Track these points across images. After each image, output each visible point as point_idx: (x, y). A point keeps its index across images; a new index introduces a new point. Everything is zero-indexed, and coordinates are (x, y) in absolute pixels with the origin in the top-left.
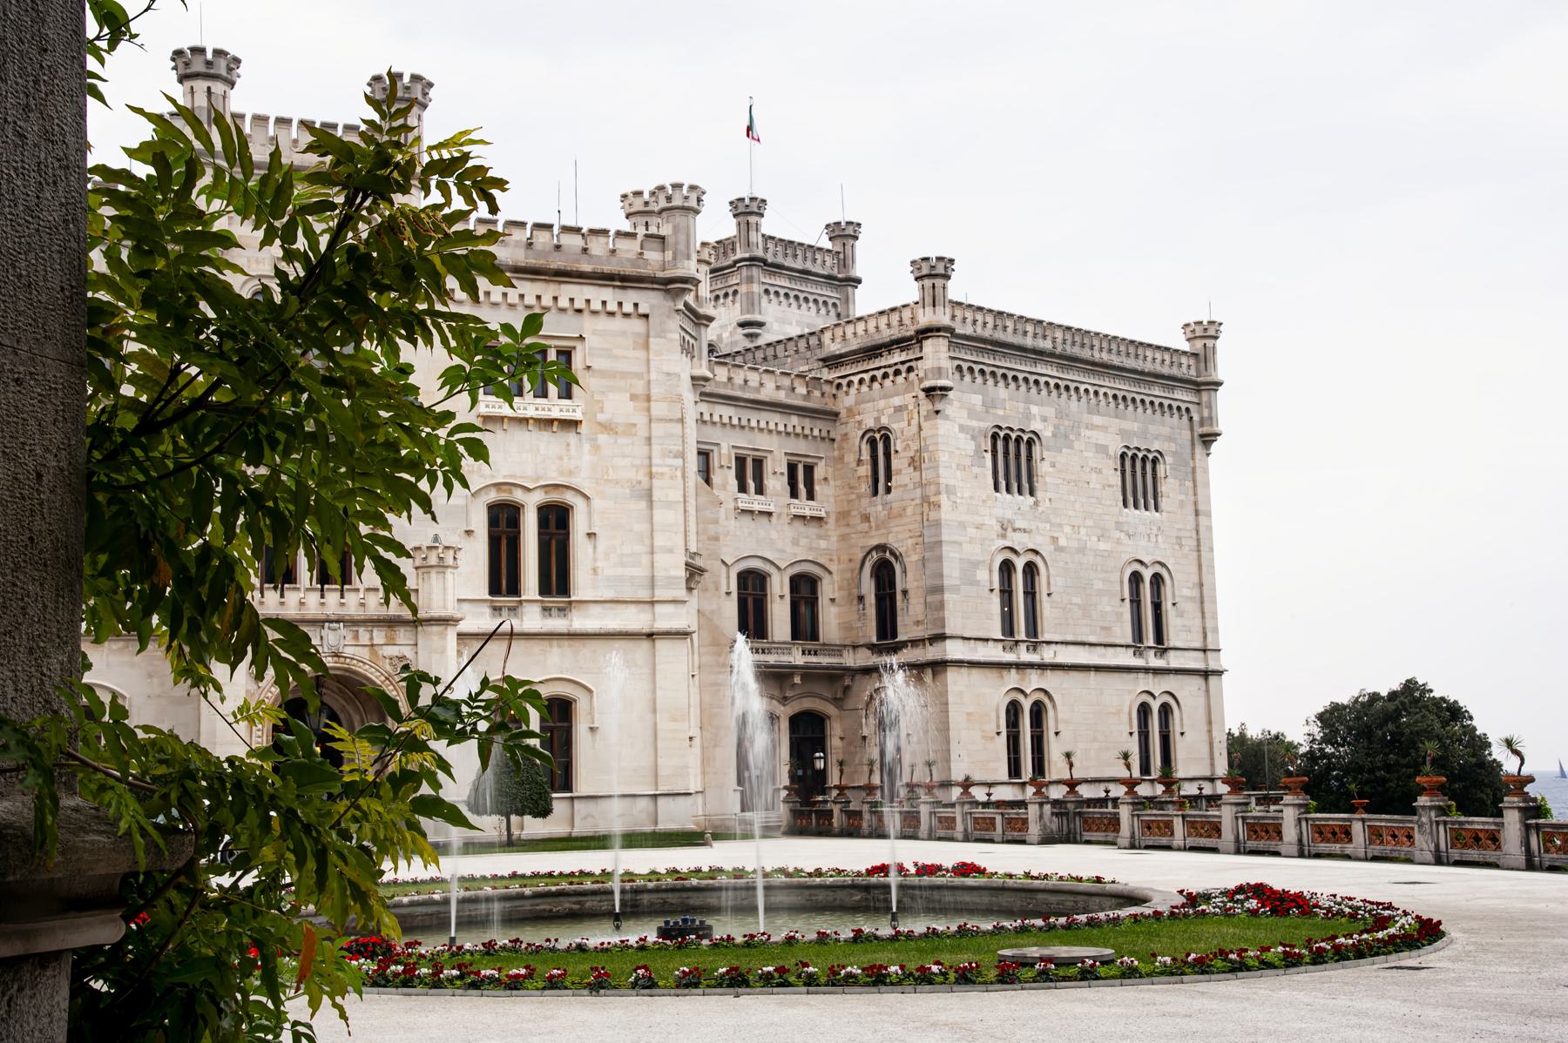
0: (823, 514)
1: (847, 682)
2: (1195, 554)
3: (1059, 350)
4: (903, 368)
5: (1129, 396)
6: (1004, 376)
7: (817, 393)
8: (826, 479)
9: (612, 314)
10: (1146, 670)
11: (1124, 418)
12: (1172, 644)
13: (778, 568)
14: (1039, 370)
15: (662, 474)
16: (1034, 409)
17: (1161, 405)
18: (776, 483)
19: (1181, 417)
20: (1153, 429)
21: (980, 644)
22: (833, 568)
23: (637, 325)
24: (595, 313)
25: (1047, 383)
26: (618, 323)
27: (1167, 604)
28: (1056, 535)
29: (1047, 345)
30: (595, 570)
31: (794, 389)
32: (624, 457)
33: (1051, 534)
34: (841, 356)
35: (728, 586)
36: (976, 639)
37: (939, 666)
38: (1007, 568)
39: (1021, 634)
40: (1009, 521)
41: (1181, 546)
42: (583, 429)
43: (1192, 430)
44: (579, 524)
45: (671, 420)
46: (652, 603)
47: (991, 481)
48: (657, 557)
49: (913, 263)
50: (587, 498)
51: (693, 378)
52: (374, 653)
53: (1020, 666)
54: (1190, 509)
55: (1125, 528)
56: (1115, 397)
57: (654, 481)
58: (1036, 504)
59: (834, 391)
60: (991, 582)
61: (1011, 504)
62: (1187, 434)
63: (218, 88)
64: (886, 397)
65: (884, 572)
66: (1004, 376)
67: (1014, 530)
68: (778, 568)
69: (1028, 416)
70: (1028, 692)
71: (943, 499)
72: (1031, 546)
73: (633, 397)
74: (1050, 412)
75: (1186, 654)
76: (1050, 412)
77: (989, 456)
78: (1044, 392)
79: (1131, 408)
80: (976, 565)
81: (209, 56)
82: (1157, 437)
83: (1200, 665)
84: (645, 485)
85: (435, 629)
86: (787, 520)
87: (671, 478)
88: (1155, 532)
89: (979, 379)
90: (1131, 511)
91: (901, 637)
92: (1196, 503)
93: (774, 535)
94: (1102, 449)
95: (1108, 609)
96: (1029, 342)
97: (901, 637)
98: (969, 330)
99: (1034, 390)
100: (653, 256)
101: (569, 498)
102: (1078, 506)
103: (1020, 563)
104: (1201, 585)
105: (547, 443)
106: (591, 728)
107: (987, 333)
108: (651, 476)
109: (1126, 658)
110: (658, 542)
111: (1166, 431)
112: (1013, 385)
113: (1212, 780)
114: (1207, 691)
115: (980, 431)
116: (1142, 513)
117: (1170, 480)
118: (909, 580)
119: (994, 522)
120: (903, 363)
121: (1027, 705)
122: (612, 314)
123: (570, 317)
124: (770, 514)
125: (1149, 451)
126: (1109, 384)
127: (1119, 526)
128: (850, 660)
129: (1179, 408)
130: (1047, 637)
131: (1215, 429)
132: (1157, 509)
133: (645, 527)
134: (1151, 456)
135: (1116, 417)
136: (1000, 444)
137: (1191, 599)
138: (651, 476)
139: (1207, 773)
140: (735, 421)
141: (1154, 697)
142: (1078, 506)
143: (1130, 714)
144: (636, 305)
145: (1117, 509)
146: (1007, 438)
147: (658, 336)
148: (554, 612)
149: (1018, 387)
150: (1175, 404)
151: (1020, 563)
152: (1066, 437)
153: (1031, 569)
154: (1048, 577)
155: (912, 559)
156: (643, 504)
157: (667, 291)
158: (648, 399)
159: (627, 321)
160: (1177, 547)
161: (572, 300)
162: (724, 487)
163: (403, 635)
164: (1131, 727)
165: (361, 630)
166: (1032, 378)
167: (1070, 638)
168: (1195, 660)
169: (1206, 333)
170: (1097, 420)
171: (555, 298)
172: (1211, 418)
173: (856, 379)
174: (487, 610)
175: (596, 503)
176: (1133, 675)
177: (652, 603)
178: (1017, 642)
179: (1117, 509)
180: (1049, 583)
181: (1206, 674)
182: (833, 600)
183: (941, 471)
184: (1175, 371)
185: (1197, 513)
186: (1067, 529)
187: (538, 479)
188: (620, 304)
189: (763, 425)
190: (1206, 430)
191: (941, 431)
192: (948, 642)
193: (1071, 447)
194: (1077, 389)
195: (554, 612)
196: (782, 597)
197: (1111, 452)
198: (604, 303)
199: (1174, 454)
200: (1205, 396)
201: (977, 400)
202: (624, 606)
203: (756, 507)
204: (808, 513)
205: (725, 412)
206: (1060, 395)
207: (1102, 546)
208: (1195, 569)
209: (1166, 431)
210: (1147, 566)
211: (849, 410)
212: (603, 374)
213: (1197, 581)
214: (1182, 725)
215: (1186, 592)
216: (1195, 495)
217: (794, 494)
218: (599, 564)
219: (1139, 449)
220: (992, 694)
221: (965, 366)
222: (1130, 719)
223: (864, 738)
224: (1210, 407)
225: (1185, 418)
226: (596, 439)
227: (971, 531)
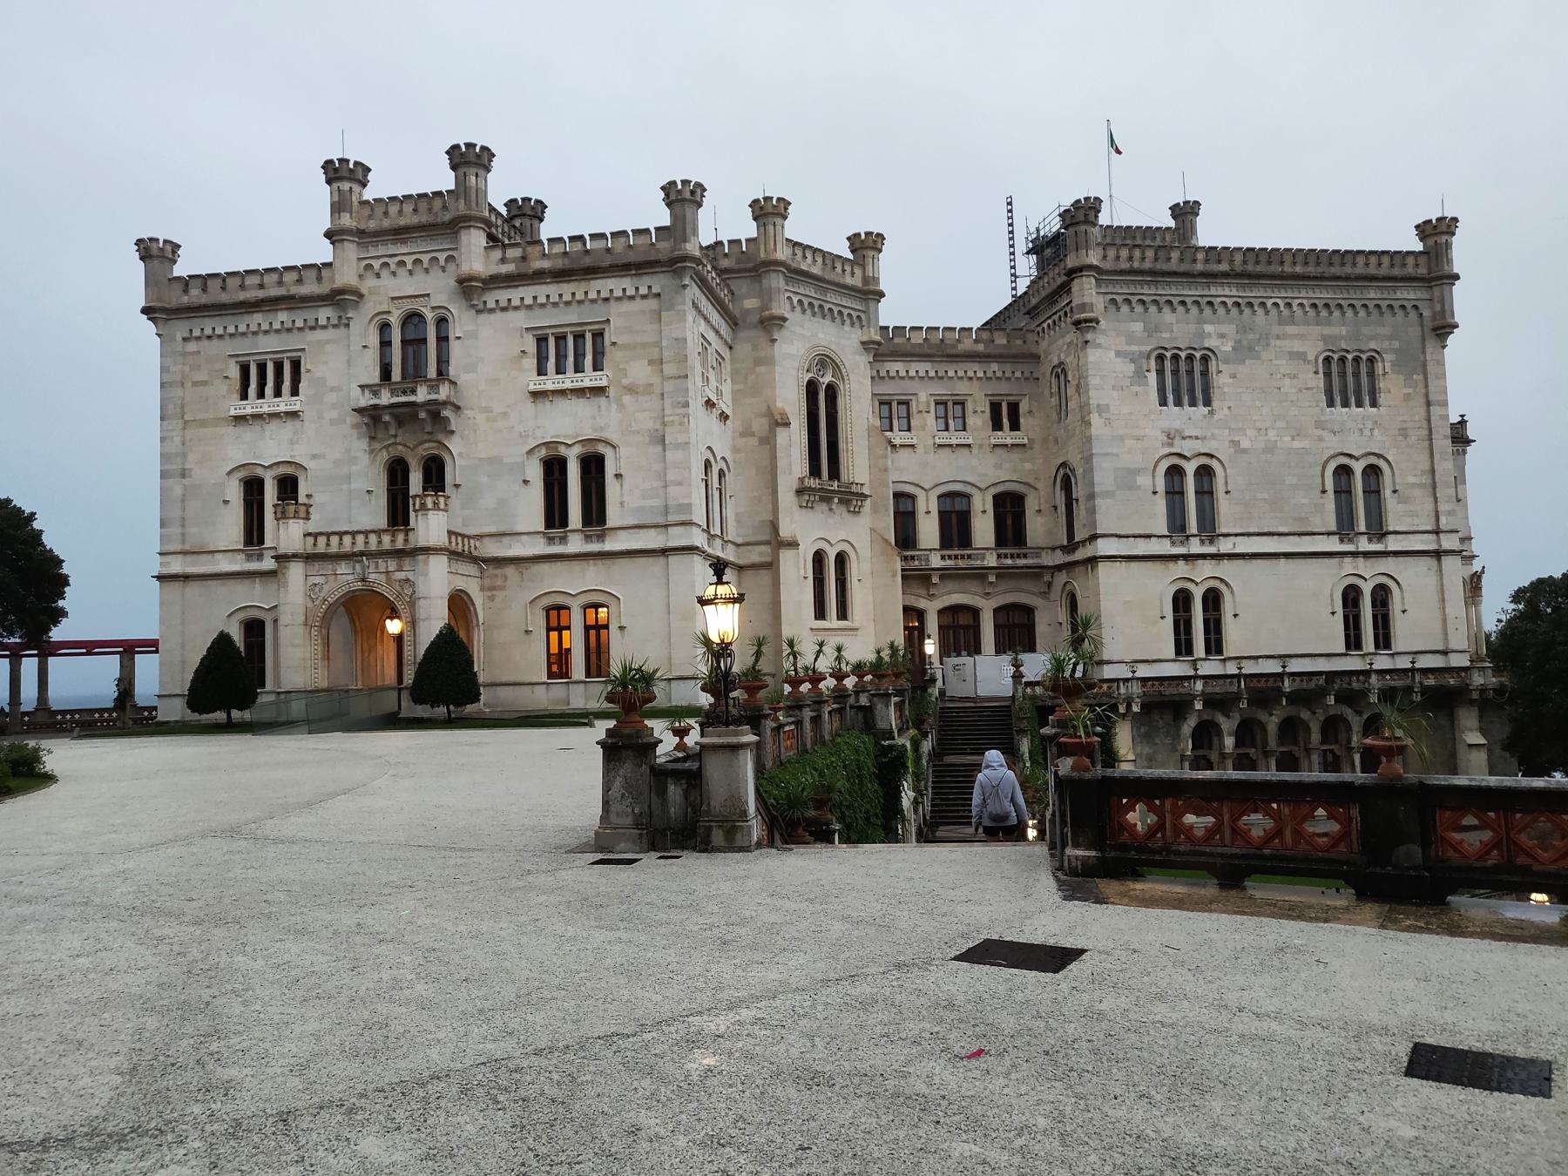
0: (1026, 441)
1: (1047, 578)
2: (1426, 443)
3: (1238, 268)
4: (1068, 309)
5: (1332, 304)
6: (1169, 302)
7: (1019, 342)
8: (1030, 412)
9: (632, 298)
10: (1354, 554)
11: (1329, 324)
12: (1391, 529)
13: (980, 489)
14: (1213, 291)
15: (672, 421)
16: (1208, 328)
17: (1378, 306)
18: (978, 420)
19: (1407, 314)
20: (1366, 330)
21: (1142, 539)
22: (1039, 485)
23: (652, 304)
24: (618, 299)
25: (1224, 303)
26: (638, 305)
27: (1387, 492)
28: (1237, 439)
29: (1224, 267)
30: (622, 504)
31: (993, 341)
32: (642, 414)
33: (1231, 438)
34: (1036, 307)
35: (927, 507)
36: (1134, 537)
37: (1093, 561)
38: (1175, 472)
39: (1193, 526)
40: (1177, 431)
41: (1406, 436)
42: (612, 392)
43: (1422, 326)
44: (610, 469)
45: (679, 377)
46: (666, 526)
47: (1154, 395)
48: (670, 489)
49: (1417, 227)
50: (615, 447)
51: (863, 343)
52: (389, 581)
53: (1188, 558)
54: (1422, 400)
55: (1329, 426)
56: (1314, 306)
57: (666, 428)
58: (1211, 413)
59: (1036, 338)
60: (1154, 486)
61: (1175, 417)
62: (1414, 331)
63: (346, 186)
64: (1063, 336)
65: (1067, 485)
66: (1169, 302)
67: (1184, 438)
68: (980, 489)
69: (1202, 335)
70: (1198, 581)
71: (1095, 419)
72: (1203, 451)
73: (651, 362)
74: (1230, 329)
75: (1411, 536)
76: (1230, 329)
77: (1152, 377)
78: (1221, 311)
79: (1337, 313)
80: (1138, 471)
81: (351, 166)
82: (1373, 338)
83: (1432, 547)
84: (661, 433)
85: (420, 557)
86: (989, 450)
87: (680, 424)
88: (1369, 425)
89: (1139, 309)
90: (1339, 410)
91: (1077, 540)
92: (1427, 395)
93: (975, 462)
94: (1301, 356)
95: (1304, 501)
96: (1199, 267)
97: (1077, 540)
98: (1125, 266)
99: (1207, 311)
100: (664, 245)
101: (602, 449)
102: (1265, 411)
103: (1190, 468)
104: (1433, 471)
105: (582, 407)
106: (622, 628)
107: (1147, 265)
108: (664, 424)
109: (1333, 545)
110: (671, 476)
111: (1386, 330)
112: (1180, 309)
113: (1445, 653)
114: (1441, 571)
115: (1141, 352)
117: (1391, 376)
118: (1079, 492)
119: (1158, 433)
120: (1067, 304)
121: (1198, 593)
122: (632, 298)
123: (600, 306)
124: (969, 446)
125: (1361, 351)
126: (1303, 295)
127: (1320, 425)
128: (1048, 559)
129: (1403, 307)
130: (1224, 530)
131: (1449, 320)
132: (1374, 404)
133: (657, 466)
134: (1364, 357)
135: (1317, 324)
136: (1168, 364)
137: (1420, 486)
138: (664, 424)
139: (1440, 648)
140: (932, 374)
141: (1366, 580)
142: (1265, 411)
143: (1332, 596)
144: (650, 287)
145: (1317, 410)
146: (1176, 357)
147: (668, 309)
148: (594, 539)
149: (1188, 311)
150: (1396, 304)
151: (1190, 468)
152: (1251, 349)
153: (1205, 473)
154: (1226, 477)
155: (1079, 472)
156: (660, 448)
157: (674, 271)
158: (662, 363)
159: (645, 302)
160: (1401, 438)
161: (599, 292)
162: (923, 428)
163: (407, 562)
164: (1333, 606)
165: (380, 561)
166: (1203, 301)
167: (1252, 530)
168: (1422, 542)
169: (1437, 232)
170: (1291, 329)
171: (586, 293)
172: (1443, 311)
173: (1045, 325)
174: (541, 540)
175: (623, 451)
176: (1335, 561)
177: (666, 526)
178: (1188, 537)
179: (1317, 410)
180: (1226, 483)
181: (1438, 554)
182: (1039, 511)
183: (1091, 393)
184: (1397, 271)
185: (1428, 404)
186: (1251, 433)
187: (577, 436)
188: (637, 289)
189: (961, 373)
190: (1439, 323)
191: (1091, 359)
192: (1099, 540)
193: (1259, 358)
194: (1263, 304)
195: (557, 540)
196: (984, 512)
197: (1311, 357)
198: (624, 290)
199: (1396, 351)
200: (1436, 291)
201: (1137, 327)
202: (645, 530)
203: (954, 441)
204: (1009, 441)
205: (922, 367)
206: (1241, 312)
207: (1297, 444)
208: (1425, 457)
209: (1386, 330)
210: (1357, 459)
211: (1045, 351)
212: (626, 347)
213: (1427, 466)
214: (1403, 604)
215: (1412, 479)
216: (1426, 386)
217: (997, 425)
218: (625, 499)
219: (1348, 351)
220: (1160, 585)
221: (1119, 299)
222: (1332, 600)
223: (1061, 624)
224: (1442, 301)
225: (1413, 315)
226: (621, 400)
227: (1129, 443)
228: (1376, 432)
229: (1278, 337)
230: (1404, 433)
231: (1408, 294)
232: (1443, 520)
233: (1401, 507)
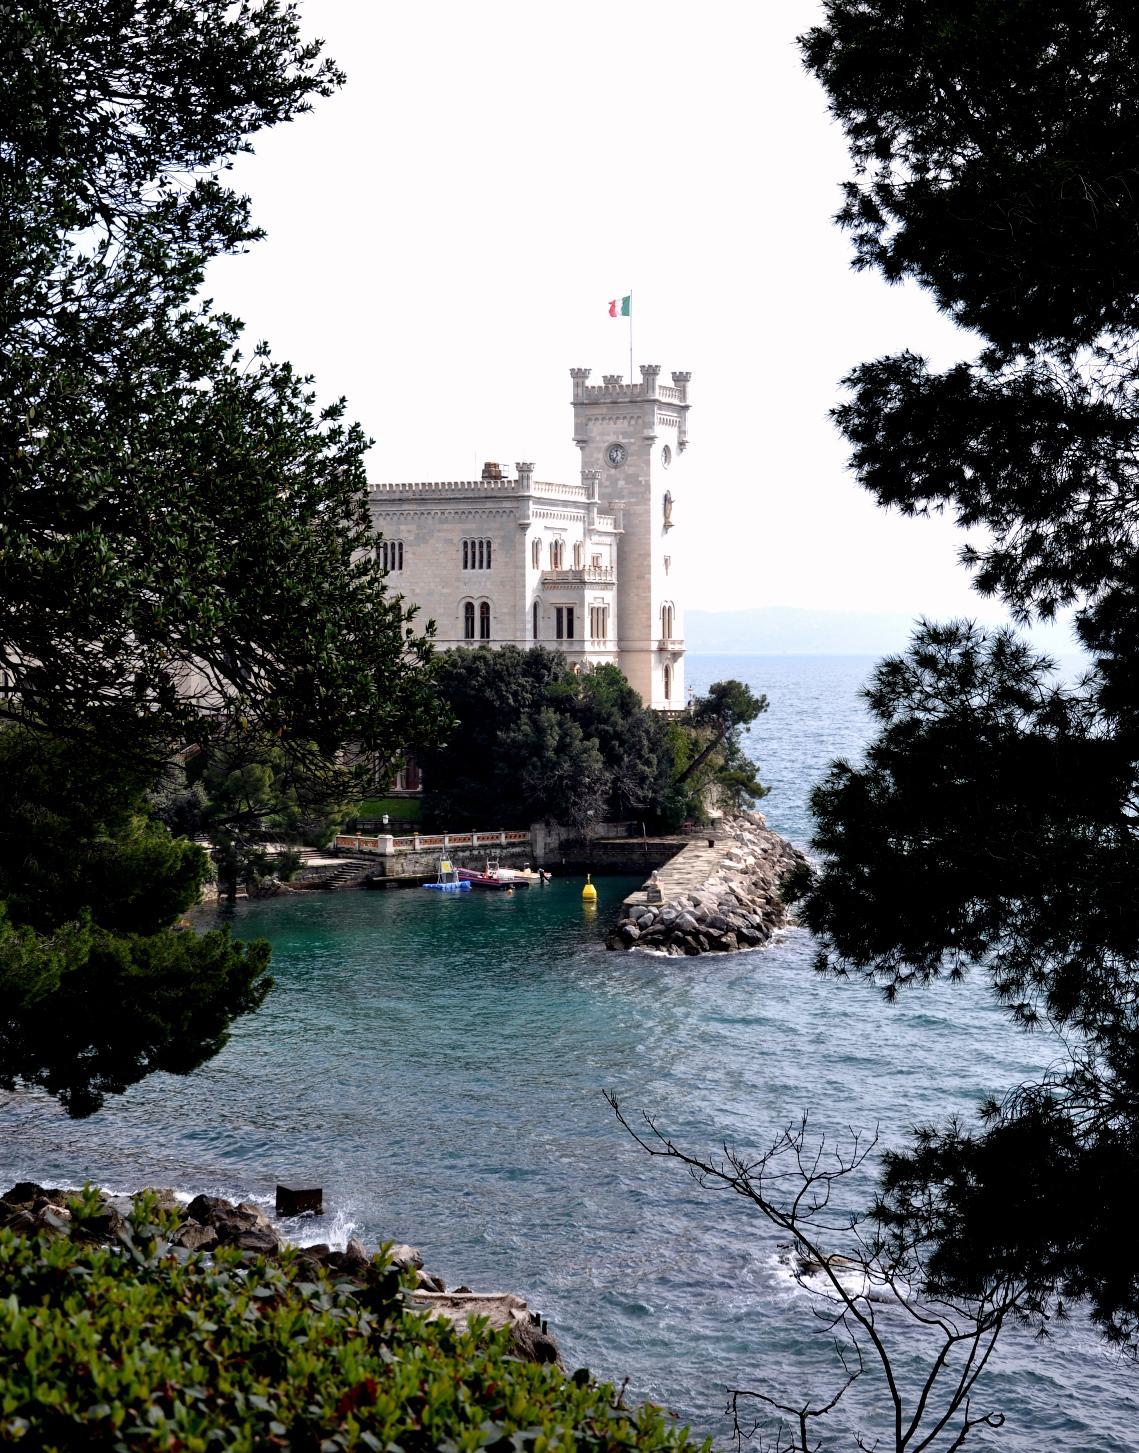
16: (403, 527)
29: (410, 495)
69: (399, 531)
74: (413, 527)
76: (413, 527)
82: (489, 530)
90: (469, 571)
94: (449, 542)
112: (388, 518)
116: (477, 570)
126: (451, 507)
127: (458, 579)
135: (461, 521)
170: (445, 526)
190: (522, 522)
207: (445, 591)
215: (505, 610)
228: (488, 583)
229: (439, 531)
230: (503, 583)
231: (507, 505)
232: (518, 634)
233: (499, 626)
